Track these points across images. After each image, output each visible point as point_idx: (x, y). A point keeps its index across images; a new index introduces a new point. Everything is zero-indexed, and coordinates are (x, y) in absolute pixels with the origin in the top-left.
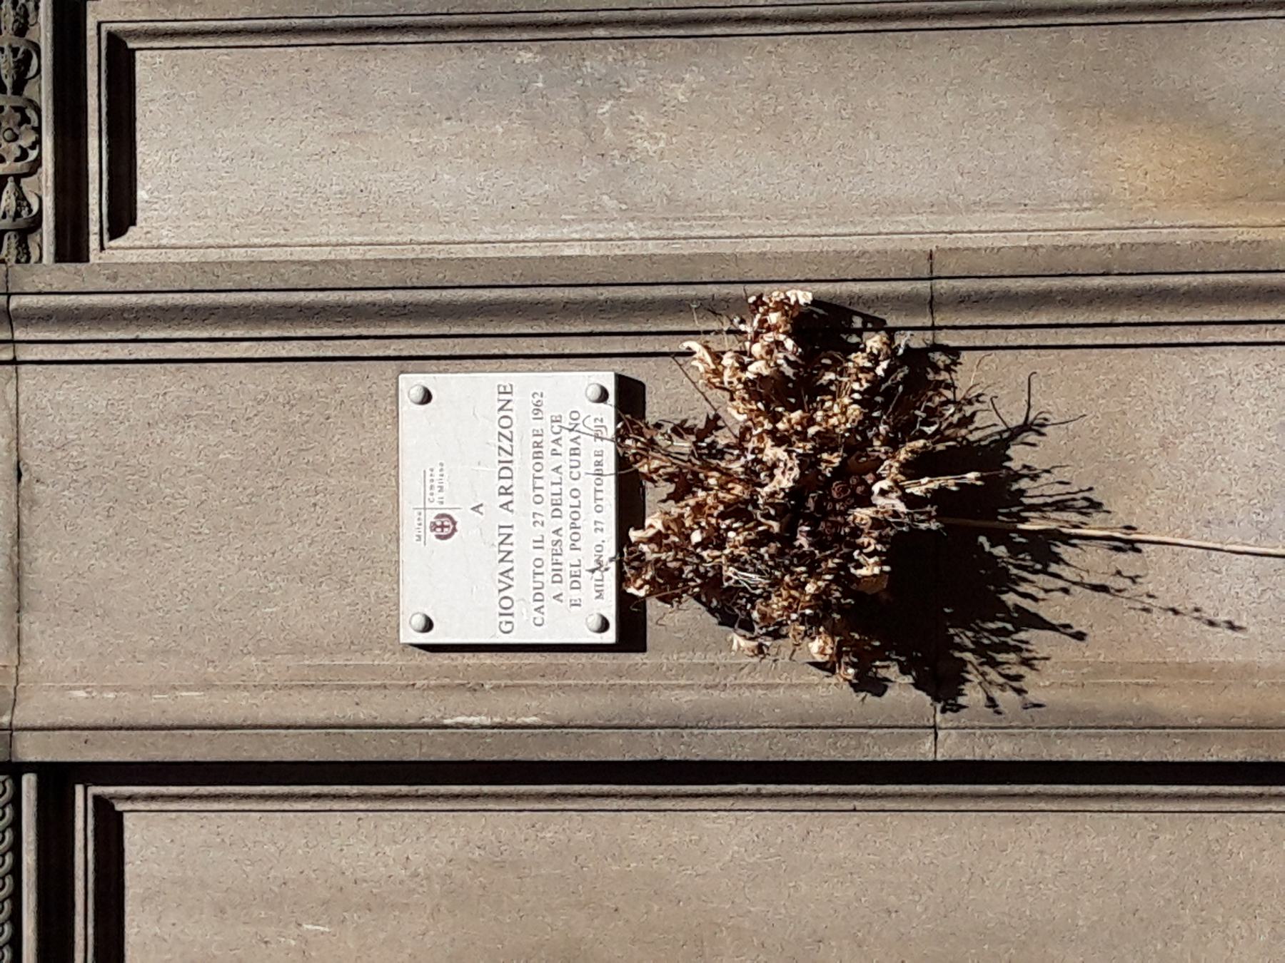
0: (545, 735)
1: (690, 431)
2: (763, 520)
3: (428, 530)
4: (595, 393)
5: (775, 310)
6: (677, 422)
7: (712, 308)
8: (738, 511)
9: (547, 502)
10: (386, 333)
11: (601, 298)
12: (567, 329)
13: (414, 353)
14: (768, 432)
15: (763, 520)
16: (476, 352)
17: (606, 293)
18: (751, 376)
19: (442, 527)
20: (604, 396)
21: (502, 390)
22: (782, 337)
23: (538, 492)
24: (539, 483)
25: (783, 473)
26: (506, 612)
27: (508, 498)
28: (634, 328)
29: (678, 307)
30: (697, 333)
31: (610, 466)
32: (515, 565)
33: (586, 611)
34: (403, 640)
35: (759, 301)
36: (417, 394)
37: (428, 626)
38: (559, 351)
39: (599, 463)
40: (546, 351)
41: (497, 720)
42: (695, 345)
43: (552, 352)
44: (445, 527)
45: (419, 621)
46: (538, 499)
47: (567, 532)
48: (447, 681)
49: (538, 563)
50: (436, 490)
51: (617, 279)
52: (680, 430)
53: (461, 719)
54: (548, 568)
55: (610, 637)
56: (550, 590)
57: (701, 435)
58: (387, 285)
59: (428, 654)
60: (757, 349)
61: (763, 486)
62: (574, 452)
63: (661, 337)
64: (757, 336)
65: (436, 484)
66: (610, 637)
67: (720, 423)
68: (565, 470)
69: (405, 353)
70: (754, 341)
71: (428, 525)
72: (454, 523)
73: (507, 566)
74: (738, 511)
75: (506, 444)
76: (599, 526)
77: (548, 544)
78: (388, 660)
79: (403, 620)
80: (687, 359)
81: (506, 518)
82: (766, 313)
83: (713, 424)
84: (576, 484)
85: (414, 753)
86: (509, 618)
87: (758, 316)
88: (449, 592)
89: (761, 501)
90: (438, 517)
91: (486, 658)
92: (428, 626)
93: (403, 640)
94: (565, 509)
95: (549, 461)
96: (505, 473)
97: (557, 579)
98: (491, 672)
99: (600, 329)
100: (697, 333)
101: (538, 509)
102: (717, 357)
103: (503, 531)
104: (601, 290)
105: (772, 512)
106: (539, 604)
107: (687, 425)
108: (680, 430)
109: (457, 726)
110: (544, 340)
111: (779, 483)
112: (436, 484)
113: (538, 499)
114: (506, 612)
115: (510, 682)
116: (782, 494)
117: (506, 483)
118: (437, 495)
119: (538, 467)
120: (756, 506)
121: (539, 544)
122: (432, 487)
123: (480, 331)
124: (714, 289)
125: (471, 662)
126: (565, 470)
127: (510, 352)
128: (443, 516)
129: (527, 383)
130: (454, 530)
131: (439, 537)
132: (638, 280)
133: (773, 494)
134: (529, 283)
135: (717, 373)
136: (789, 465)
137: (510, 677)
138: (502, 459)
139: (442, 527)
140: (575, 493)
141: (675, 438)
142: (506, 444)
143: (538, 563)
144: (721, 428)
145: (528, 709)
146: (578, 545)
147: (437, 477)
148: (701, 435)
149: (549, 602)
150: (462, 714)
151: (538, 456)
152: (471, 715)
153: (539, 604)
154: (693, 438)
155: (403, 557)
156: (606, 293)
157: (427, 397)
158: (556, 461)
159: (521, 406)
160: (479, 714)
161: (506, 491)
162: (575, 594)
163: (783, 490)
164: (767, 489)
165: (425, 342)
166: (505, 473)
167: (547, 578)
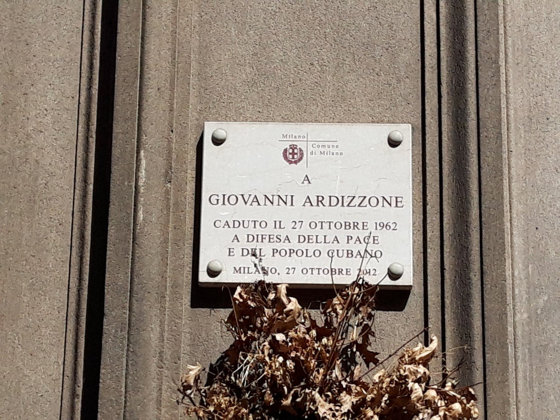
0: (129, 225)
1: (366, 339)
2: (292, 392)
3: (291, 143)
4: (397, 269)
5: (464, 409)
6: (373, 330)
7: (464, 363)
8: (300, 375)
9: (313, 233)
10: (443, 116)
11: (472, 275)
12: (446, 250)
13: (427, 136)
14: (364, 399)
15: (292, 392)
16: (428, 182)
17: (475, 279)
19: (293, 154)
20: (394, 276)
21: (399, 200)
22: (441, 413)
23: (319, 225)
24: (326, 226)
25: (331, 409)
26: (226, 199)
27: (314, 203)
28: (447, 301)
29: (464, 334)
30: (444, 349)
31: (339, 280)
32: (262, 207)
33: (226, 258)
34: (206, 123)
35: (471, 397)
36: (397, 136)
37: (217, 142)
38: (429, 244)
39: (340, 271)
40: (429, 235)
41: (142, 190)
42: (434, 345)
43: (428, 240)
44: (293, 155)
45: (221, 134)
46: (313, 225)
47: (287, 246)
48: (174, 156)
49: (263, 224)
50: (322, 150)
51: (487, 287)
52: (367, 332)
53: (143, 162)
54: (259, 231)
55: (204, 277)
56: (242, 233)
57: (362, 348)
58: (480, 114)
59: (196, 144)
60: (432, 393)
61: (320, 393)
62: (350, 254)
63: (440, 323)
64: (443, 395)
65: (326, 149)
66: (204, 277)
67: (372, 365)
68: (335, 246)
69: (427, 129)
70: (438, 392)
71: (294, 143)
72: (296, 162)
73: (262, 202)
74: (300, 375)
75: (357, 201)
76: (291, 271)
77: (277, 232)
78: (193, 115)
79: (224, 125)
80: (423, 340)
81: (299, 200)
82: (461, 403)
83: (371, 359)
84: (324, 255)
85: (118, 128)
86: (221, 202)
87: (459, 396)
88: (243, 160)
89: (307, 391)
90: (301, 150)
92: (217, 142)
93: (206, 123)
94: (304, 246)
95: (342, 234)
96: (334, 201)
97: (251, 238)
98: (180, 189)
99: (447, 275)
100: (444, 349)
101: (306, 224)
102: (425, 362)
103: (289, 198)
104: (478, 276)
105: (298, 400)
106: (231, 225)
107: (370, 336)
108: (367, 332)
109: (138, 160)
110: (438, 233)
111: (323, 406)
112: (326, 149)
113: (313, 225)
114: (226, 199)
115: (172, 202)
116: (314, 408)
117: (326, 201)
118: (318, 150)
119: (338, 225)
120: (303, 388)
121: (278, 225)
122: (324, 146)
123: (445, 186)
124: (479, 362)
125: (189, 176)
126: (335, 246)
127: (428, 207)
128: (302, 154)
129: (405, 217)
130: (291, 162)
131: (286, 150)
132: (486, 303)
133: (313, 401)
134: (483, 219)
135: (413, 361)
136: (337, 414)
137: (176, 204)
138: (345, 198)
139: (293, 154)
140: (317, 253)
141: (361, 327)
142: (357, 201)
143: (263, 224)
144: (368, 366)
145: (149, 214)
146: (277, 255)
147: (331, 150)
148: (362, 348)
149: (232, 232)
150: (147, 164)
151: (347, 225)
152: (145, 170)
153: (231, 225)
154: (360, 342)
155: (271, 126)
156: (475, 279)
157: (394, 143)
158: (343, 239)
159: (387, 214)
160: (148, 178)
161: (320, 201)
162: (237, 252)
163: (317, 409)
164: (317, 396)
165: (436, 145)
166: (334, 201)
167: (252, 231)
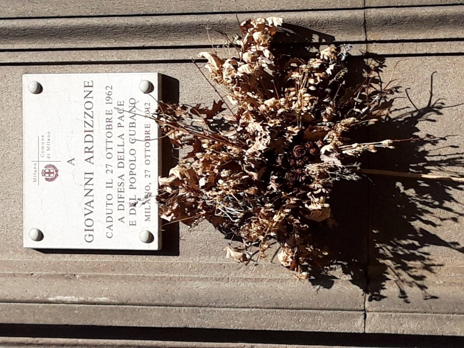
0: (111, 308)
1: (202, 111)
2: (247, 171)
3: (41, 175)
4: (145, 86)
5: (258, 30)
6: (195, 105)
7: (220, 30)
8: (232, 165)
9: (115, 156)
10: (15, 48)
11: (148, 23)
12: (128, 45)
13: (33, 61)
14: (252, 112)
15: (247, 171)
16: (72, 60)
17: (152, 21)
18: (240, 75)
19: (49, 173)
20: (150, 88)
21: (86, 84)
22: (262, 48)
23: (109, 151)
24: (110, 145)
25: (260, 140)
26: (89, 229)
27: (90, 155)
28: (170, 44)
29: (197, 29)
30: (210, 47)
31: (154, 134)
32: (94, 198)
33: (139, 227)
34: (25, 246)
35: (248, 24)
36: (33, 87)
37: (40, 237)
38: (124, 59)
39: (147, 133)
40: (116, 59)
41: (82, 299)
42: (206, 54)
43: (119, 60)
44: (51, 173)
45: (34, 234)
46: (109, 156)
47: (127, 177)
48: (53, 272)
49: (109, 197)
50: (46, 149)
51: (158, 11)
52: (197, 111)
53: (59, 298)
54: (115, 201)
55: (154, 246)
56: (116, 215)
57: (210, 114)
58: (13, 16)
59: (42, 254)
60: (246, 57)
61: (247, 148)
62: (132, 125)
63: (188, 50)
64: (247, 47)
65: (45, 146)
66: (154, 246)
67: (224, 106)
68: (126, 137)
69: (27, 61)
70: (245, 51)
71: (40, 172)
72: (57, 171)
73: (90, 199)
74: (232, 165)
75: (89, 120)
76: (148, 173)
77: (115, 185)
78: (18, 258)
79: (26, 232)
80: (203, 64)
81: (88, 167)
82: (253, 32)
83: (218, 107)
84: (133, 146)
85: (30, 320)
86: (91, 233)
87: (248, 34)
88: (56, 214)
89: (246, 159)
90: (46, 167)
91: (78, 257)
92: (40, 237)
93: (25, 246)
94: (127, 163)
95: (116, 131)
96: (89, 138)
97: (121, 207)
98: (81, 267)
99: (149, 44)
100: (210, 47)
101: (109, 162)
102: (221, 62)
103: (87, 176)
104: (149, 18)
105: (253, 166)
106: (110, 224)
107: (200, 108)
108: (197, 111)
109: (57, 302)
110: (114, 52)
111: (258, 146)
112: (45, 146)
113: (109, 156)
114: (89, 229)
115: (92, 273)
116: (260, 153)
117: (89, 145)
118: (46, 152)
119: (109, 135)
120: (243, 162)
121: (109, 185)
122: (43, 148)
123: (73, 46)
124: (220, 17)
125: (70, 259)
126: (126, 137)
127: (93, 60)
128: (50, 166)
129: (101, 79)
130: (57, 175)
131: (47, 179)
132: (170, 12)
133: (254, 154)
134: (101, 14)
135: (220, 72)
136: (264, 135)
137: (93, 270)
138: (86, 129)
139: (49, 173)
140: (133, 152)
141: (194, 116)
142: (89, 120)
143: (109, 197)
144: (225, 109)
145: (101, 291)
146: (134, 185)
147: (46, 141)
148: (210, 114)
149: (116, 223)
150: (60, 295)
151: (109, 127)
152: (65, 295)
153: (110, 224)
154: (205, 116)
155: (26, 192)
156: (152, 21)
157: (39, 89)
158: (120, 131)
159: (98, 95)
160: (71, 294)
161: (89, 150)
162: (132, 218)
163: (260, 151)
164: (250, 151)
165: (40, 53)
166: (89, 138)
167: (115, 207)
